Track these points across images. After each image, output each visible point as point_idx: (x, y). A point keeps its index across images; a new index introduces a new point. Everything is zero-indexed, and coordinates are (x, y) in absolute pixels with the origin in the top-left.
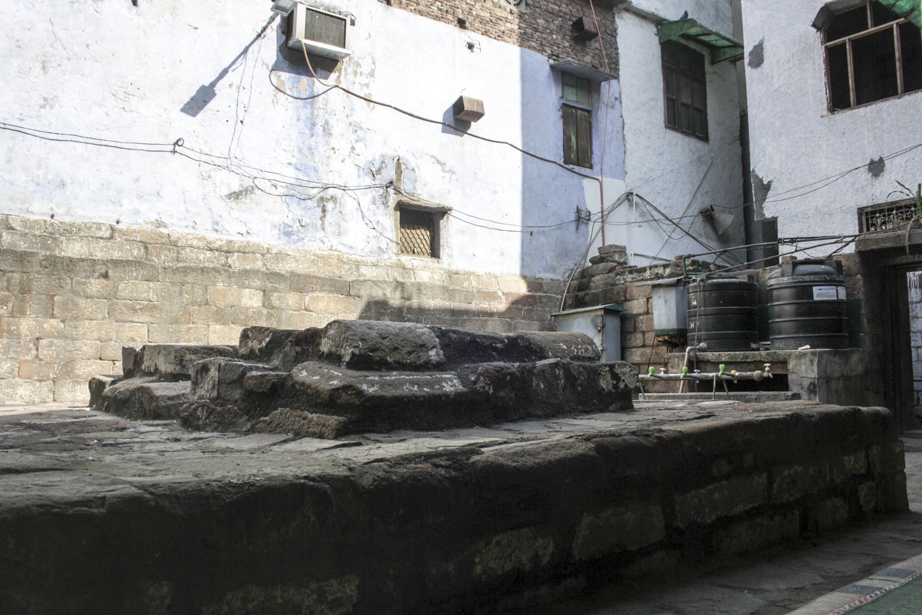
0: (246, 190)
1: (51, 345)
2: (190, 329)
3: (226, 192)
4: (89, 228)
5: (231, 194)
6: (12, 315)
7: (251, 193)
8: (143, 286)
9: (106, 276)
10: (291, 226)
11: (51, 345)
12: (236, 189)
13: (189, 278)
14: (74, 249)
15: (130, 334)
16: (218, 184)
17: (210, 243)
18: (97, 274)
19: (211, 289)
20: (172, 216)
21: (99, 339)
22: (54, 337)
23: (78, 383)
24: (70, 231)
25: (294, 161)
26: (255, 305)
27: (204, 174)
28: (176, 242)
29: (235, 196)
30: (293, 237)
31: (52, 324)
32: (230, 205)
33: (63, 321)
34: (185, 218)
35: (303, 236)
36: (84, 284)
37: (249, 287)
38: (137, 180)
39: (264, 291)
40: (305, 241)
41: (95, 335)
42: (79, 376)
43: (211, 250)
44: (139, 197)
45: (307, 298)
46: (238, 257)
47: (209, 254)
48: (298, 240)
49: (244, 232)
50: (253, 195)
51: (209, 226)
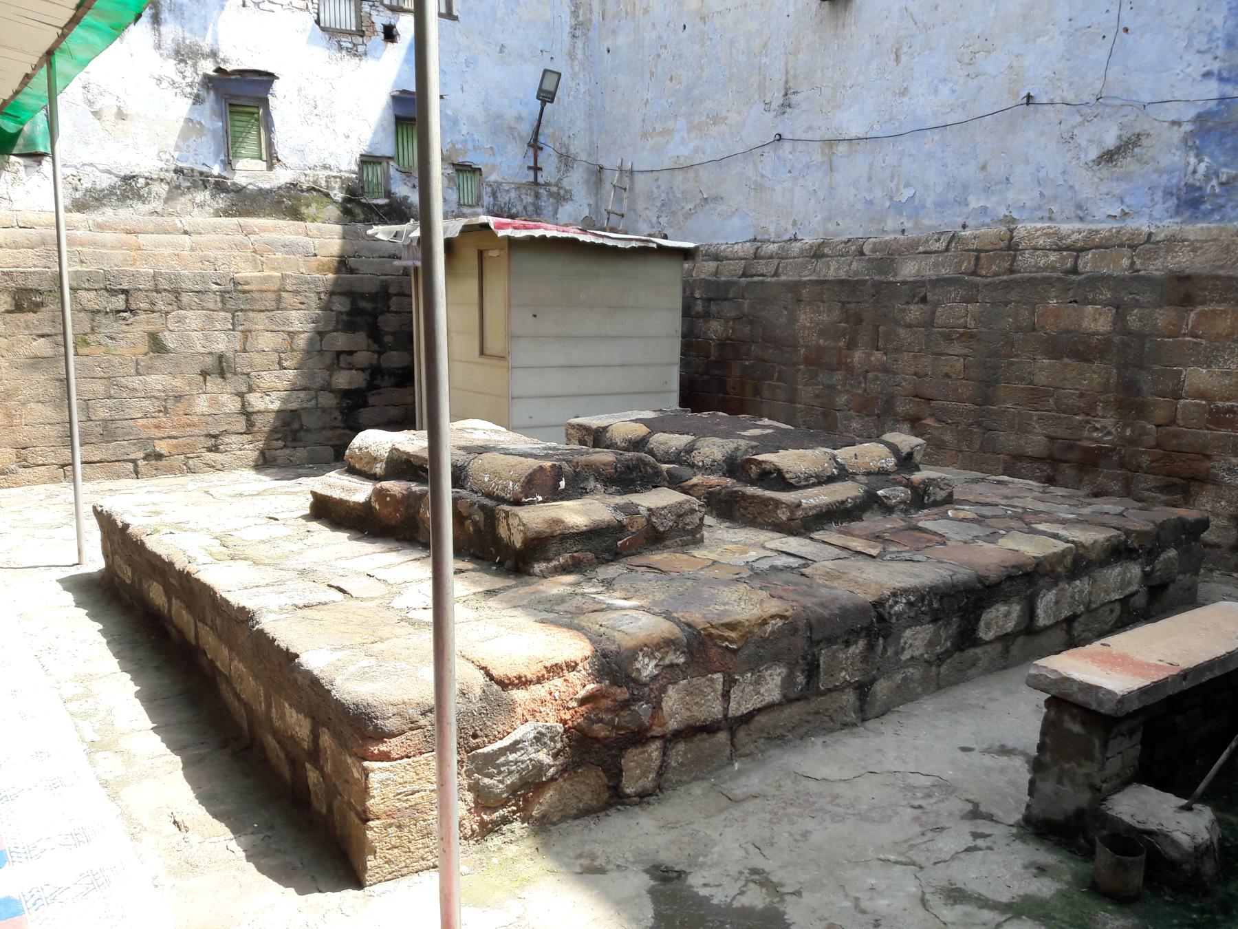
0: (1127, 143)
1: (877, 378)
2: (1012, 363)
3: (1093, 154)
4: (927, 241)
5: (1101, 157)
6: (849, 348)
7: (1135, 145)
8: (959, 308)
9: (924, 300)
10: (1200, 188)
11: (877, 378)
12: (1110, 141)
13: (1013, 296)
14: (909, 270)
15: (946, 369)
16: (1084, 144)
17: (1061, 239)
18: (917, 299)
19: (1040, 308)
20: (1024, 206)
21: (915, 374)
22: (878, 370)
23: (898, 421)
24: (913, 248)
25: (1215, 66)
26: (1101, 329)
27: (1065, 135)
28: (1017, 244)
29: (1109, 157)
30: (1203, 207)
31: (878, 356)
32: (1098, 174)
33: (885, 354)
34: (1039, 208)
35: (1221, 201)
36: (904, 311)
37: (1094, 303)
38: (984, 168)
39: (1118, 308)
40: (1228, 209)
41: (913, 369)
42: (898, 414)
43: (1060, 249)
44: (987, 190)
45: (1192, 315)
46: (1094, 255)
47: (1053, 257)
48: (1212, 211)
49: (1116, 211)
50: (1136, 150)
51: (1070, 211)
